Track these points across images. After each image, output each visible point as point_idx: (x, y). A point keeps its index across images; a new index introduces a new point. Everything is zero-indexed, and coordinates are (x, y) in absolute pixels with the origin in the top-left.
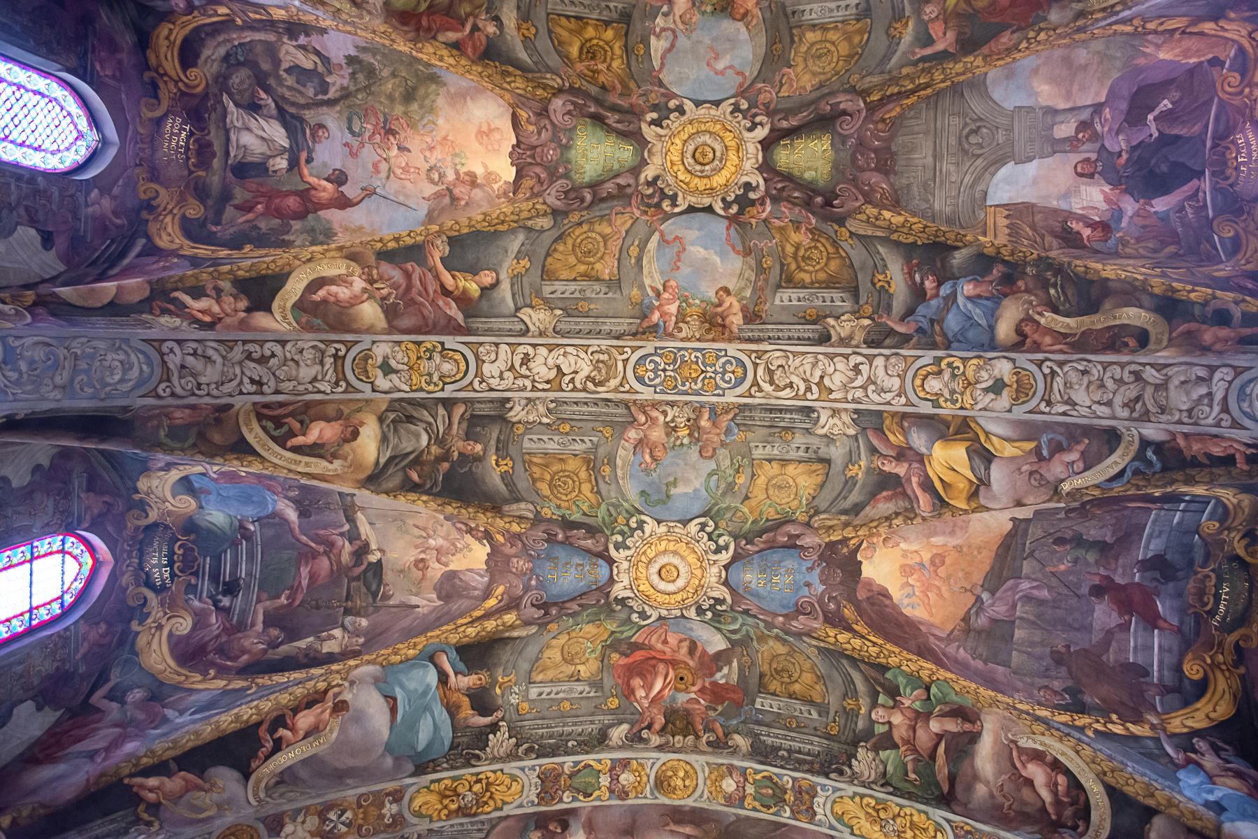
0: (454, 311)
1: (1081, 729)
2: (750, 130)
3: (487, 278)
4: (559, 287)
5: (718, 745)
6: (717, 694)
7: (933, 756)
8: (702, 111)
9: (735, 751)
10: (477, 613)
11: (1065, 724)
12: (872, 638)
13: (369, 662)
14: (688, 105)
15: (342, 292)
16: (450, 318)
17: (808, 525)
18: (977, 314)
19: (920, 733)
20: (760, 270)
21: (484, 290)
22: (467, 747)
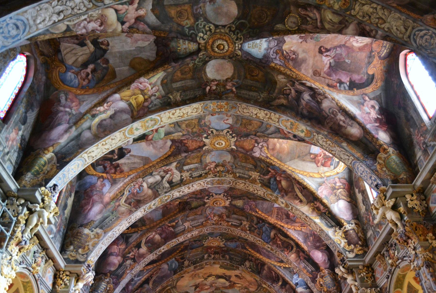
0: (172, 229)
1: (280, 267)
2: (227, 200)
3: (176, 221)
4: (190, 218)
5: (223, 257)
6: (223, 251)
7: (258, 264)
8: (217, 196)
9: (226, 260)
10: (180, 249)
11: (278, 266)
12: (249, 250)
13: (164, 262)
14: (214, 195)
15: (151, 236)
16: (171, 231)
17: (238, 240)
18: (268, 229)
19: (257, 261)
20: (229, 211)
21: (176, 223)
22: (181, 267)
